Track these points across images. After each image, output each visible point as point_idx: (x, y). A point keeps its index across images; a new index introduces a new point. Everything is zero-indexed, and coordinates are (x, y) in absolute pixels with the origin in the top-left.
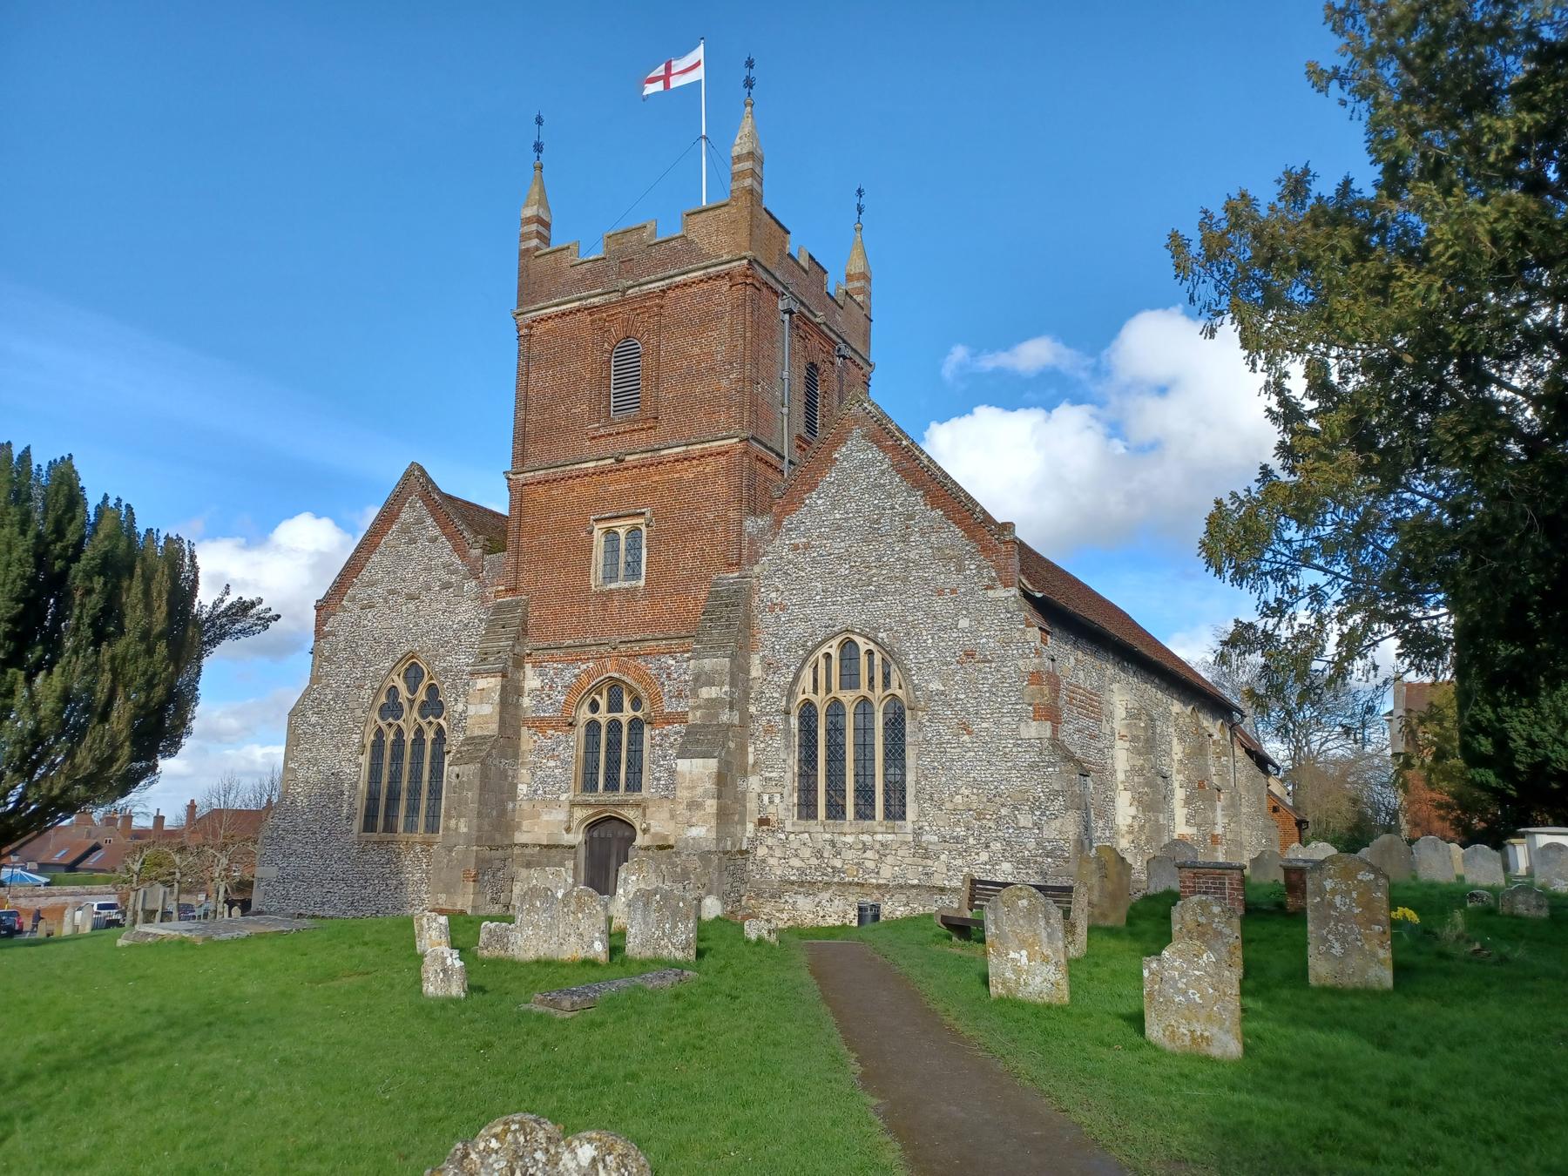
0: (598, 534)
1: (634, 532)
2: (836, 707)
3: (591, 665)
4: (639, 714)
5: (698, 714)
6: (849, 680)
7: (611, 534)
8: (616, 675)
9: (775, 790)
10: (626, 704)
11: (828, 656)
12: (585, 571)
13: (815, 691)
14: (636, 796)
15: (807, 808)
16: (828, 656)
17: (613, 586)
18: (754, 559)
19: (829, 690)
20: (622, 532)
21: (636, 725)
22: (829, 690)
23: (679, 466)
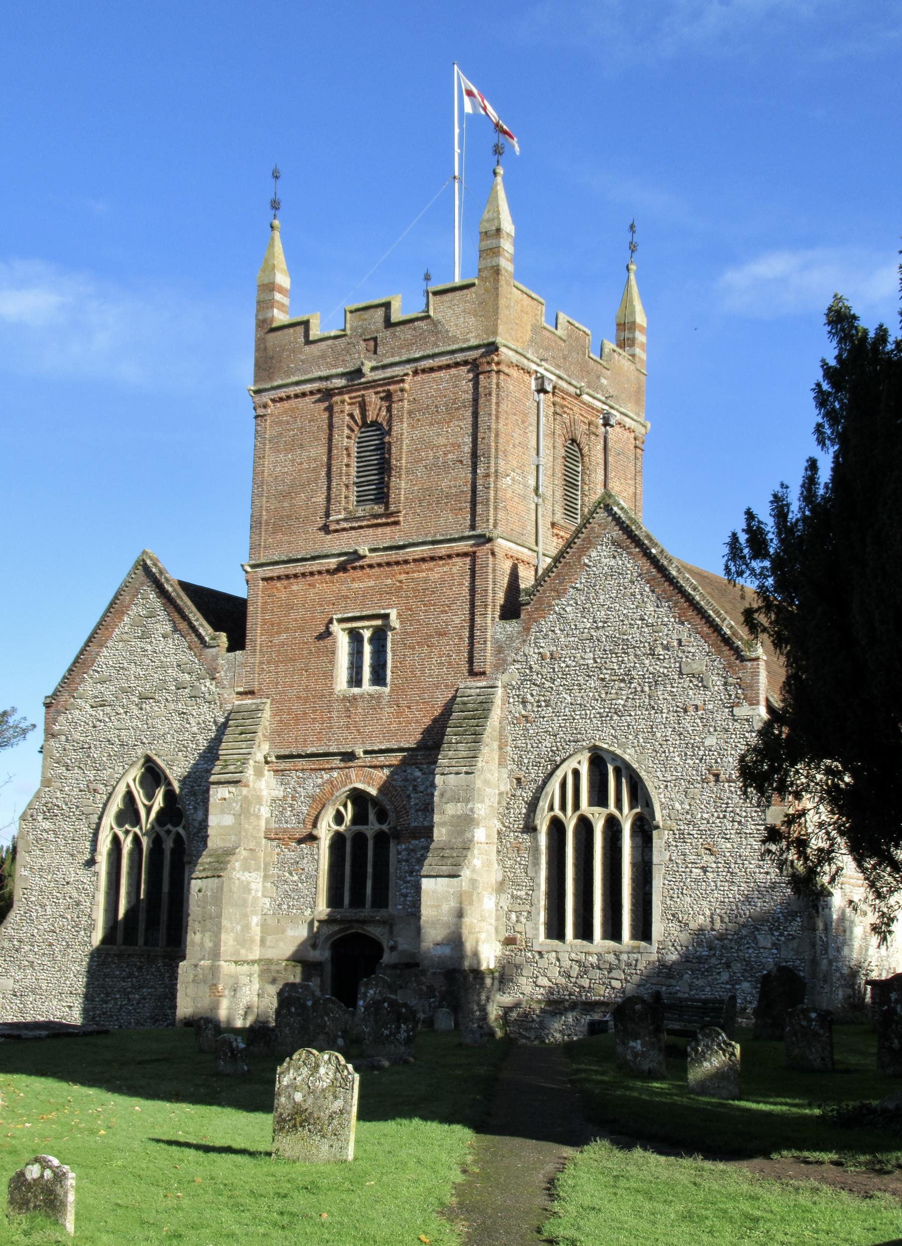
2: (585, 825)
3: (335, 774)
4: (385, 827)
5: (444, 830)
6: (599, 797)
7: (355, 637)
8: (360, 786)
9: (522, 907)
11: (576, 773)
12: (329, 675)
13: (563, 808)
15: (556, 930)
17: (356, 690)
19: (577, 806)
23: (424, 566)
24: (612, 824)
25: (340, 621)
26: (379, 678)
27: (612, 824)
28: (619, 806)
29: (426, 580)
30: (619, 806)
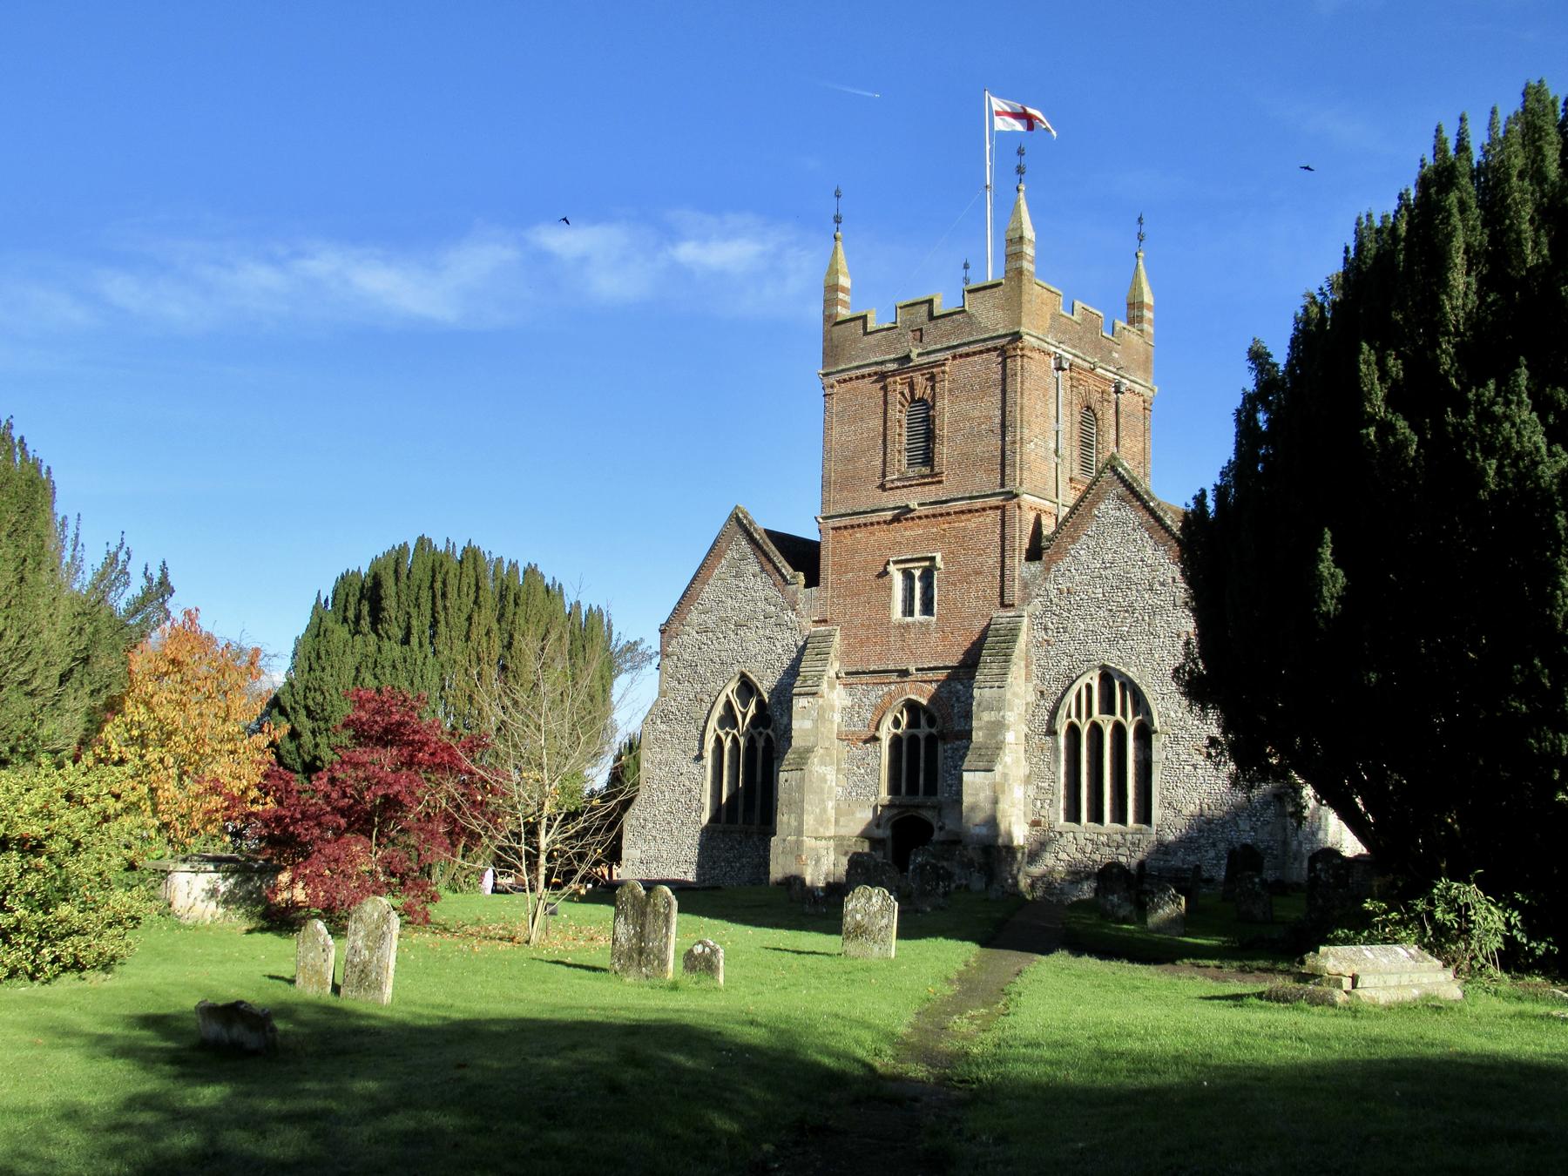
0: (898, 579)
1: (927, 576)
2: (1096, 730)
4: (934, 731)
6: (1108, 707)
7: (908, 575)
8: (913, 697)
10: (923, 721)
11: (1089, 687)
12: (887, 606)
13: (1079, 715)
14: (931, 801)
16: (1089, 687)
17: (909, 619)
18: (1026, 599)
19: (1089, 714)
20: (917, 573)
21: (931, 740)
22: (1089, 714)
24: (1119, 730)
25: (896, 562)
26: (927, 608)
27: (1119, 730)
28: (1124, 714)
29: (965, 529)
30: (1124, 714)
